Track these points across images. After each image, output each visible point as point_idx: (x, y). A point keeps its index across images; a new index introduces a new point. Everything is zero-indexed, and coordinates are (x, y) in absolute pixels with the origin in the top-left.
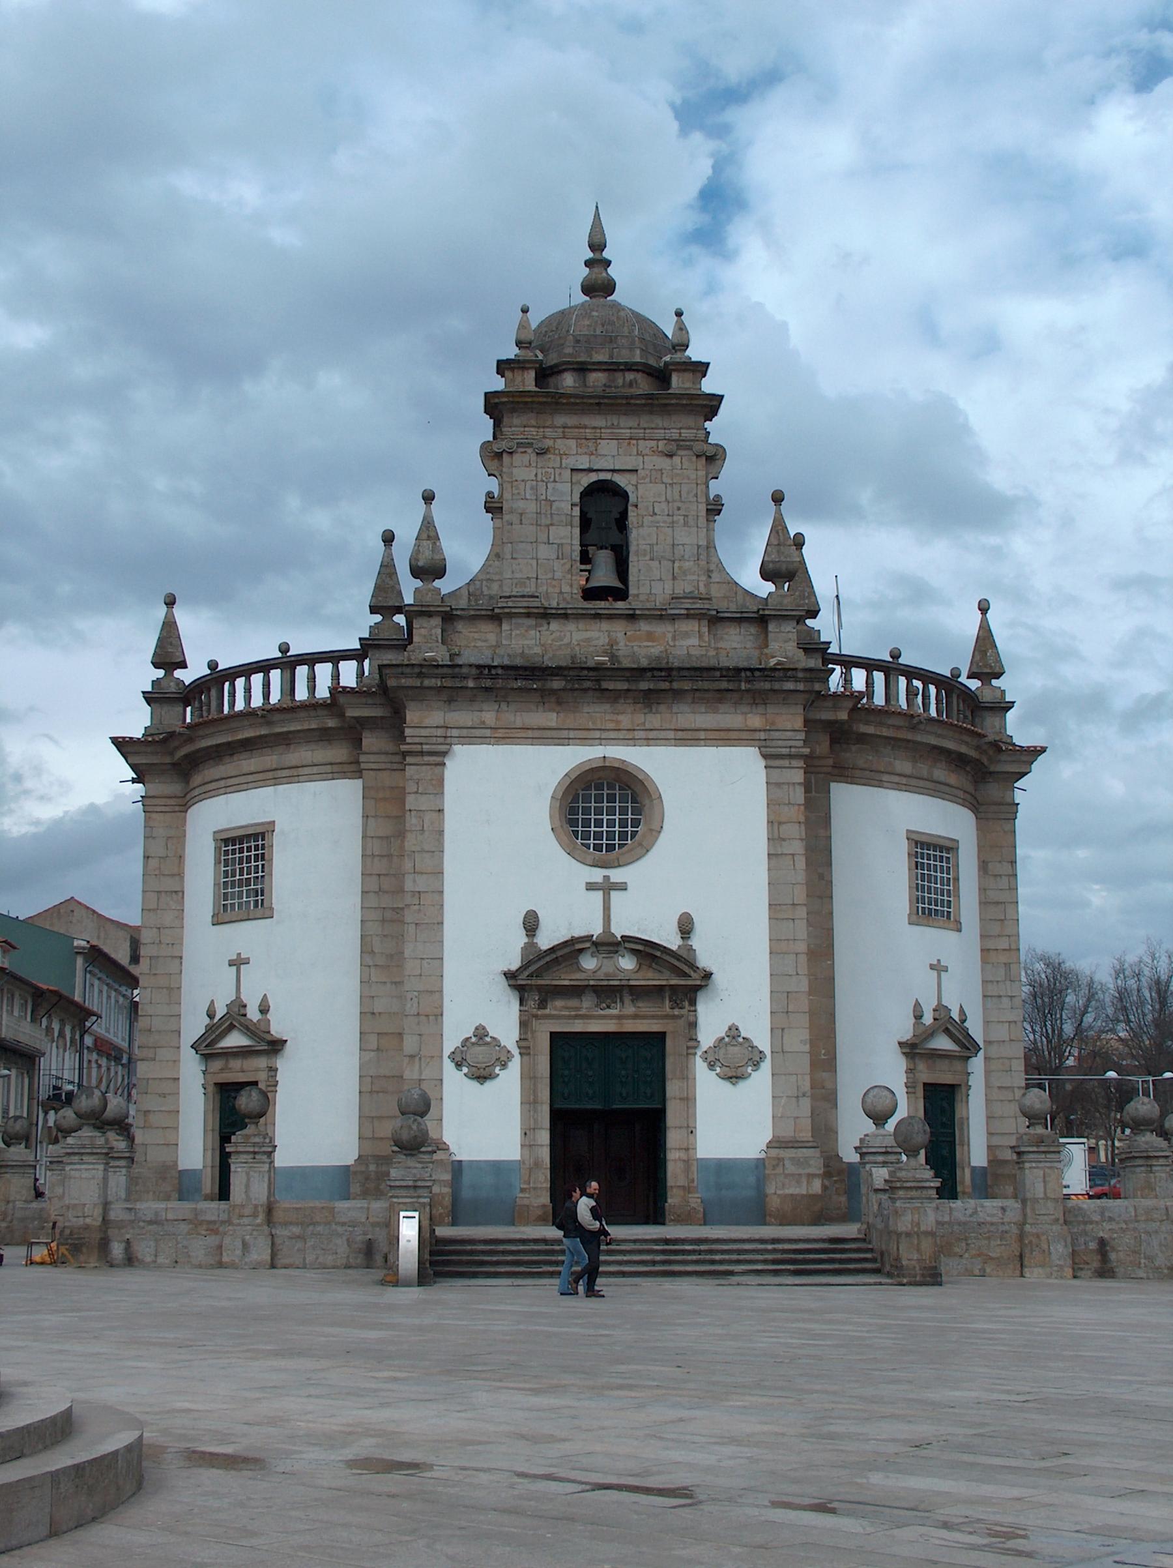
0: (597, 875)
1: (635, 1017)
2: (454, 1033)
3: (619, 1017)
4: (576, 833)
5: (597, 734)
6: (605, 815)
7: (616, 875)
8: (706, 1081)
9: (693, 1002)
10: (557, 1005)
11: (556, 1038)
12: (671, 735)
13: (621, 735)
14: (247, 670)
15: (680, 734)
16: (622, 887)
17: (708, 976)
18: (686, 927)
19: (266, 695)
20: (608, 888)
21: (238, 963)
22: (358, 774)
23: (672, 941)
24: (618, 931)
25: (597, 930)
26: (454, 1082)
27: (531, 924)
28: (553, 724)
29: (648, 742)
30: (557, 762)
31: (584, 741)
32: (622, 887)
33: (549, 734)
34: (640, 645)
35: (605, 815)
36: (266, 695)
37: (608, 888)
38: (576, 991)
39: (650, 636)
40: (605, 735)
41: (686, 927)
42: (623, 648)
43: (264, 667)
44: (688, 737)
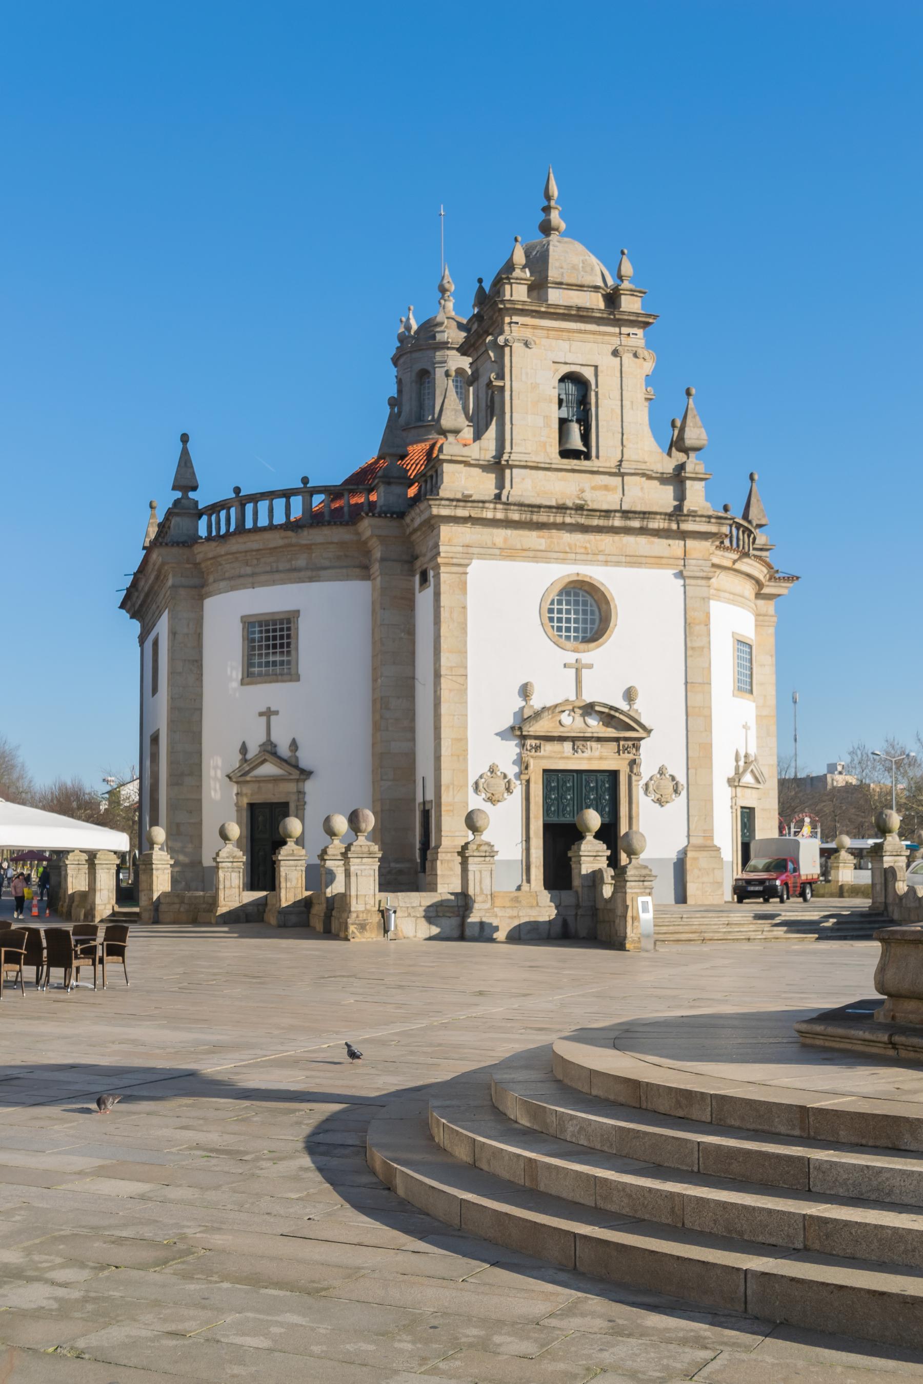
0: (571, 657)
1: (601, 758)
2: (476, 768)
3: (590, 759)
4: (553, 627)
5: (573, 556)
7: (586, 658)
8: (644, 804)
9: (638, 748)
10: (548, 748)
11: (548, 773)
12: (623, 559)
13: (590, 557)
14: (271, 495)
15: (628, 559)
16: (590, 666)
17: (649, 731)
19: (288, 514)
22: (367, 577)
23: (624, 706)
24: (588, 697)
25: (572, 697)
28: (543, 548)
29: (606, 563)
31: (563, 561)
32: (590, 666)
33: (539, 554)
34: (602, 494)
36: (288, 514)
38: (562, 739)
39: (606, 488)
40: (578, 557)
42: (588, 496)
43: (287, 494)
44: (635, 561)
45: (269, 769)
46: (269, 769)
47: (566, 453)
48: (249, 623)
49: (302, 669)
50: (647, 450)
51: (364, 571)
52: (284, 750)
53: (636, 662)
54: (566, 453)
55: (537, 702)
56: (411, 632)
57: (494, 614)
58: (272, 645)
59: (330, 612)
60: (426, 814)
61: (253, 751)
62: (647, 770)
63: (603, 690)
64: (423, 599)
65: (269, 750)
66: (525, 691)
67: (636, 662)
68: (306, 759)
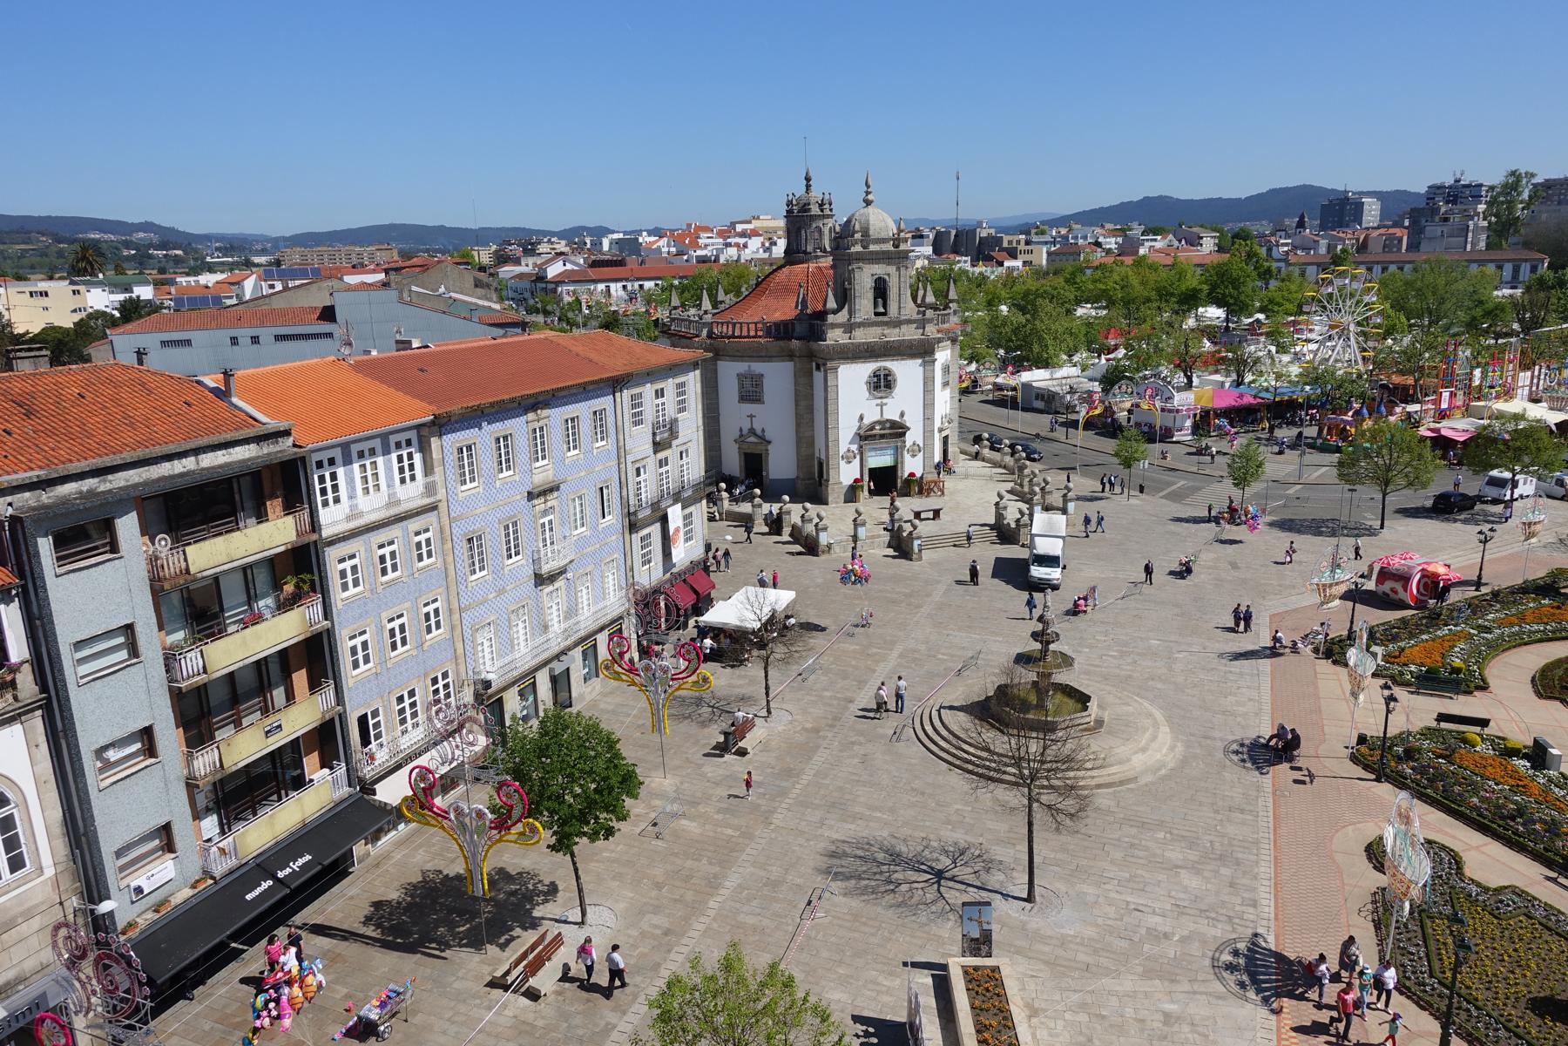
6: (882, 384)
18: (902, 415)
20: (882, 406)
21: (751, 416)
26: (842, 463)
27: (861, 418)
30: (865, 369)
34: (893, 335)
35: (882, 384)
37: (882, 406)
41: (902, 415)
45: (752, 439)
46: (752, 439)
47: (877, 314)
48: (741, 377)
49: (766, 398)
50: (910, 310)
51: (790, 356)
52: (759, 432)
53: (904, 402)
54: (877, 314)
55: (867, 421)
56: (812, 386)
57: (851, 395)
58: (751, 392)
59: (778, 376)
60: (821, 464)
61: (745, 431)
62: (908, 444)
63: (892, 414)
64: (818, 376)
65: (752, 431)
66: (861, 418)
67: (904, 402)
68: (768, 436)
